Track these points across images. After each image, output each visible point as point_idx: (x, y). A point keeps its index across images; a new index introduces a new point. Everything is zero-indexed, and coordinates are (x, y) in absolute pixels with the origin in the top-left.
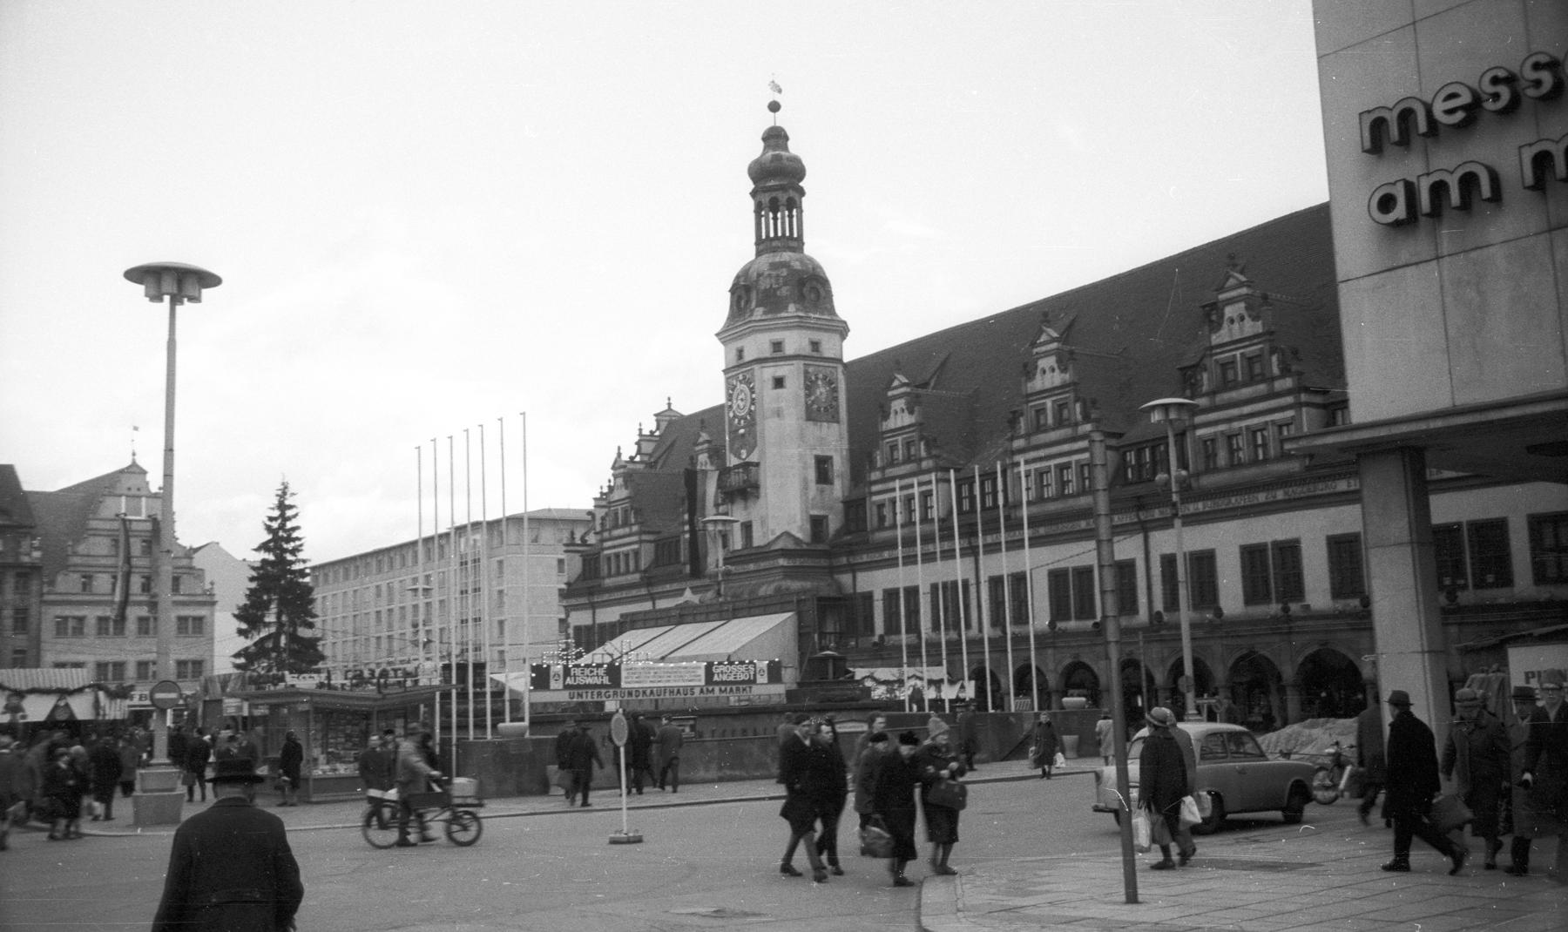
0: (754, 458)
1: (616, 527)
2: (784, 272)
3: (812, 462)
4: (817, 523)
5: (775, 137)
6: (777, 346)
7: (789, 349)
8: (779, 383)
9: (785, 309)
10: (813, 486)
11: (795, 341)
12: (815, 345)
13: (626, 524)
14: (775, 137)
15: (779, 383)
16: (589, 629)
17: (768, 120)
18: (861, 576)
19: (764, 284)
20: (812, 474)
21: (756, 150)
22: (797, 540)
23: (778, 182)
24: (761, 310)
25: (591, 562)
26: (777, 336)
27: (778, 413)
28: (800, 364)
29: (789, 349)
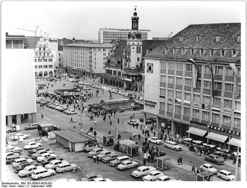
0: (130, 57)
1: (112, 57)
2: (135, 34)
3: (137, 58)
4: (137, 66)
5: (135, 14)
6: (134, 44)
7: (135, 44)
8: (133, 48)
9: (135, 39)
10: (137, 61)
11: (136, 43)
12: (138, 44)
13: (114, 57)
14: (135, 14)
15: (133, 48)
16: (109, 70)
17: (134, 11)
18: (142, 73)
19: (133, 35)
20: (137, 60)
21: (132, 16)
22: (135, 68)
23: (135, 20)
24: (132, 38)
25: (109, 61)
26: (134, 42)
27: (133, 52)
28: (136, 46)
29: (135, 44)
